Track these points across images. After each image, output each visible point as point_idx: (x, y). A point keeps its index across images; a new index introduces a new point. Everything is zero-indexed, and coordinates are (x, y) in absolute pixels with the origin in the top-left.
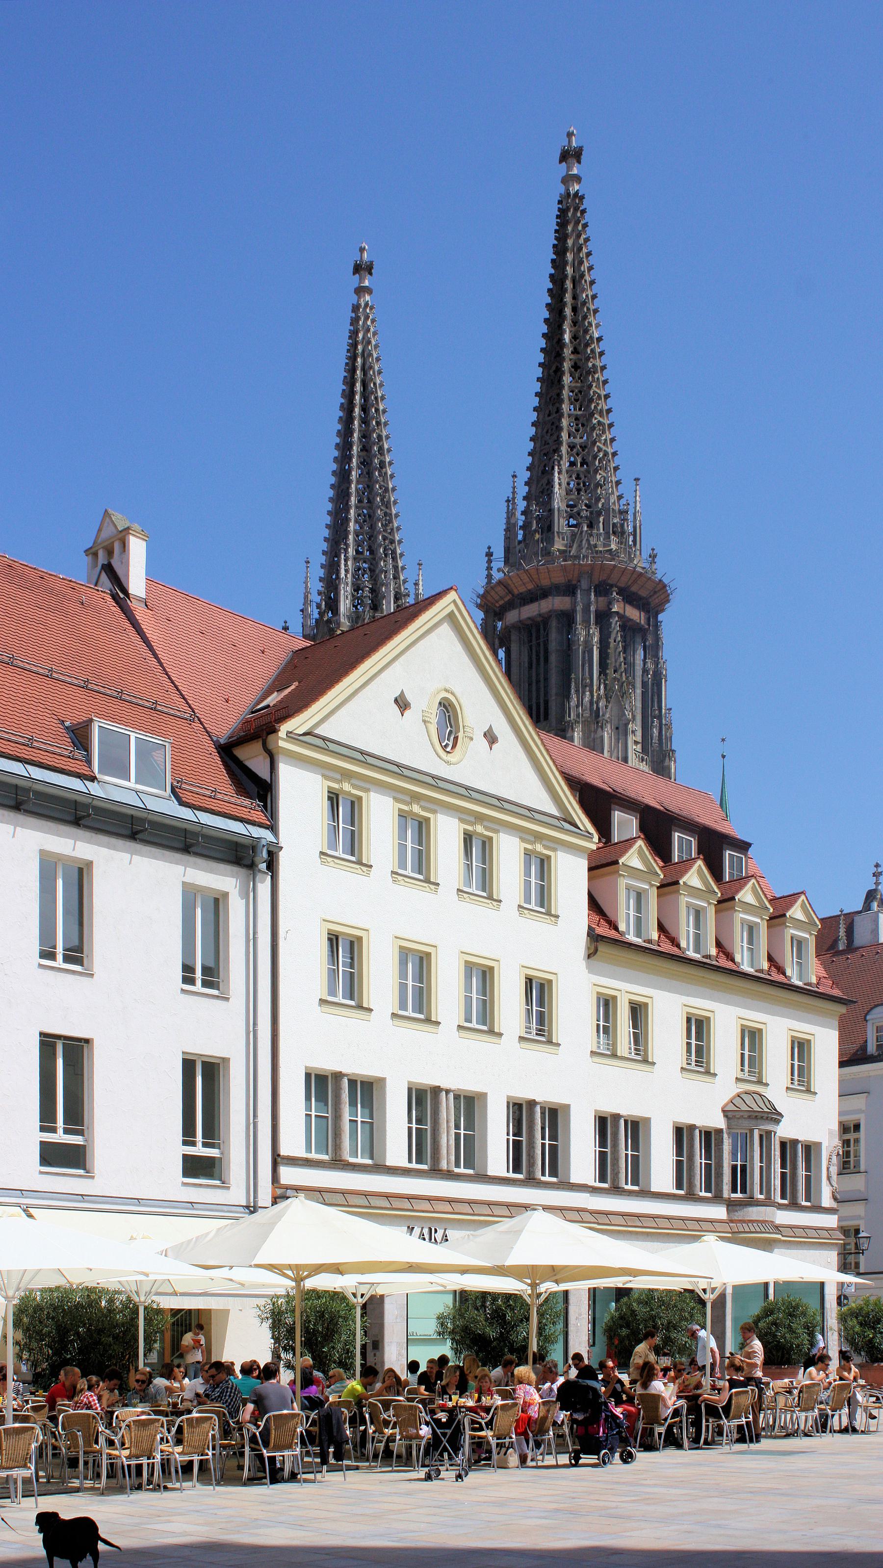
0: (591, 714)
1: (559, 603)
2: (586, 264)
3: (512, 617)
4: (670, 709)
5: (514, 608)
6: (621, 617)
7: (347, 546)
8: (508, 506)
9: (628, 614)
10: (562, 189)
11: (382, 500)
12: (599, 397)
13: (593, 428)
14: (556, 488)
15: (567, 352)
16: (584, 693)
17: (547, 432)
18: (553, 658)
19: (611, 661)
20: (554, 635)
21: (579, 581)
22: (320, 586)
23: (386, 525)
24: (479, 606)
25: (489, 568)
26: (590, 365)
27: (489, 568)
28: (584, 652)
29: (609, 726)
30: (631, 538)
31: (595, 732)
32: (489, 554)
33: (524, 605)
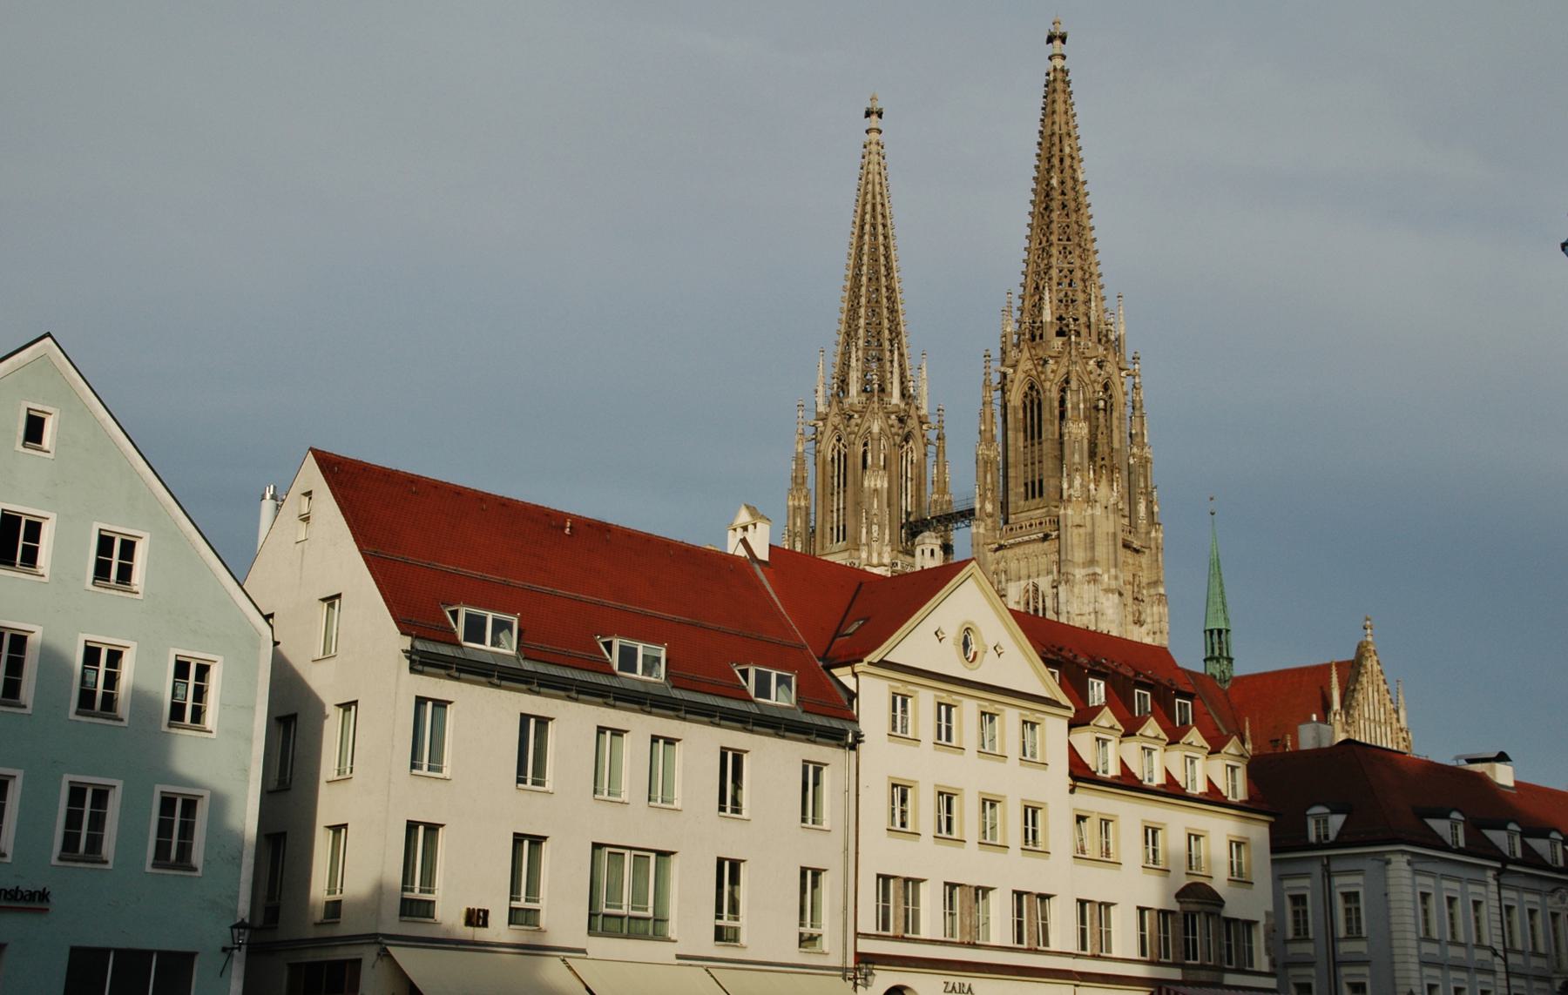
15: (1056, 194)
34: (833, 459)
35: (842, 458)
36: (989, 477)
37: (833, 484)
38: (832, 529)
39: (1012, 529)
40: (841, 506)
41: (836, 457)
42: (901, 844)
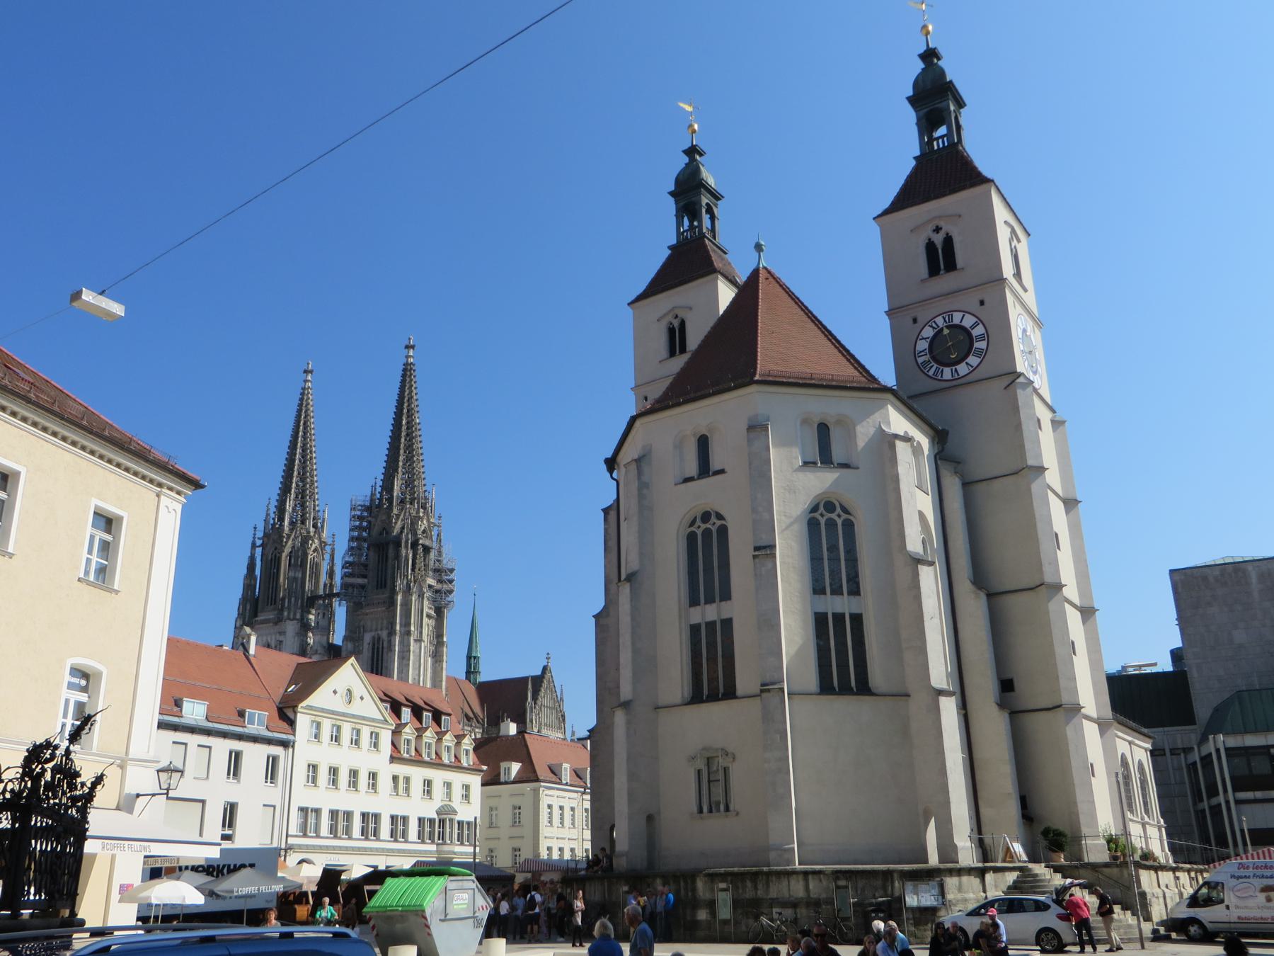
6: (423, 545)
7: (291, 494)
11: (310, 475)
12: (418, 448)
14: (396, 488)
19: (417, 566)
26: (414, 435)
34: (272, 559)
41: (273, 558)
42: (312, 791)
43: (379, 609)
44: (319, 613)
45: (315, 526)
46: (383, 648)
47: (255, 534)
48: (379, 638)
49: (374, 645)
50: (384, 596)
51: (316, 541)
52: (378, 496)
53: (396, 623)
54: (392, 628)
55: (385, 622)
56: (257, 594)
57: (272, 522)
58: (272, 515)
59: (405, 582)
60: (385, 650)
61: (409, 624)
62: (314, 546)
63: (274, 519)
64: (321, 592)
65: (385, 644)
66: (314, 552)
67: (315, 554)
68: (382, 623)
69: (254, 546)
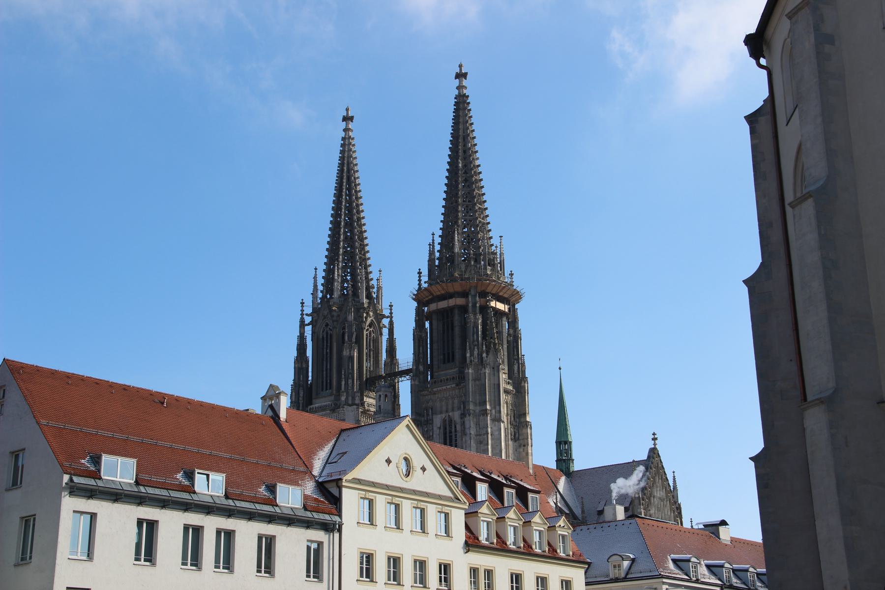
0: (478, 360)
1: (460, 301)
2: (469, 122)
3: (433, 307)
4: (524, 355)
5: (434, 302)
7: (338, 261)
8: (430, 247)
9: (497, 307)
10: (456, 92)
13: (476, 211)
16: (474, 349)
17: (451, 212)
18: (457, 330)
20: (457, 318)
21: (470, 291)
22: (323, 281)
23: (361, 251)
24: (414, 299)
25: (420, 280)
26: (474, 179)
27: (420, 280)
28: (474, 328)
29: (489, 366)
30: (499, 265)
31: (481, 370)
32: (420, 273)
33: (440, 301)
34: (323, 337)
35: (329, 337)
36: (421, 349)
37: (323, 353)
38: (323, 382)
39: (435, 382)
40: (328, 367)
41: (325, 336)
43: (448, 387)
44: (380, 396)
45: (369, 296)
46: (456, 431)
47: (302, 311)
48: (451, 421)
49: (445, 429)
50: (453, 371)
51: (371, 314)
52: (437, 255)
53: (469, 401)
54: (464, 407)
55: (456, 401)
56: (310, 378)
57: (320, 295)
58: (320, 288)
59: (476, 352)
60: (459, 434)
61: (484, 403)
62: (369, 320)
63: (322, 292)
64: (383, 373)
65: (459, 427)
66: (370, 326)
67: (371, 329)
68: (453, 403)
69: (302, 324)
